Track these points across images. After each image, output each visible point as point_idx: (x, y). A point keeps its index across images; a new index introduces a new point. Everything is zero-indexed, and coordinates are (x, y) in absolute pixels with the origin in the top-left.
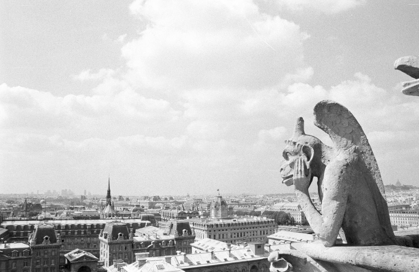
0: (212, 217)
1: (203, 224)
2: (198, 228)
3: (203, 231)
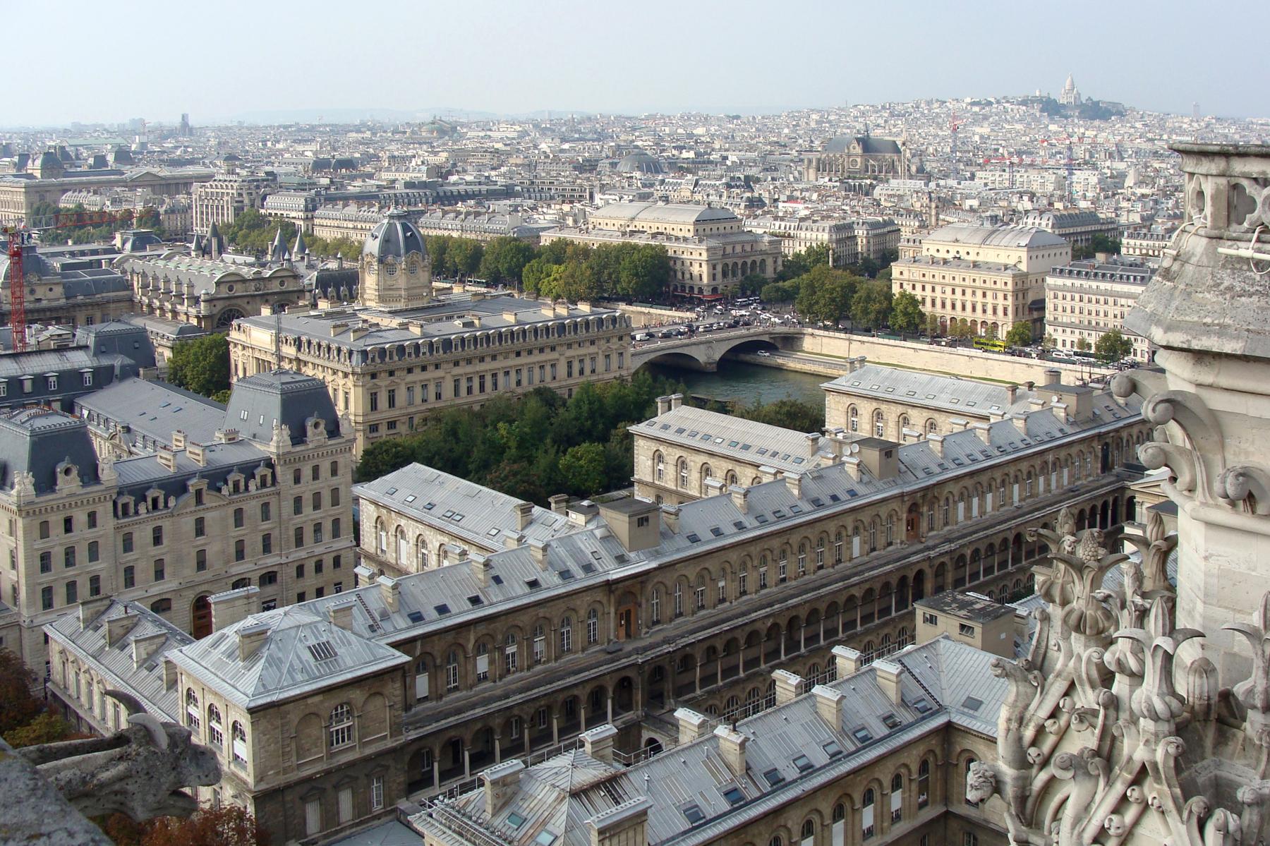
0: (368, 304)
1: (345, 349)
2: (317, 361)
3: (346, 375)
